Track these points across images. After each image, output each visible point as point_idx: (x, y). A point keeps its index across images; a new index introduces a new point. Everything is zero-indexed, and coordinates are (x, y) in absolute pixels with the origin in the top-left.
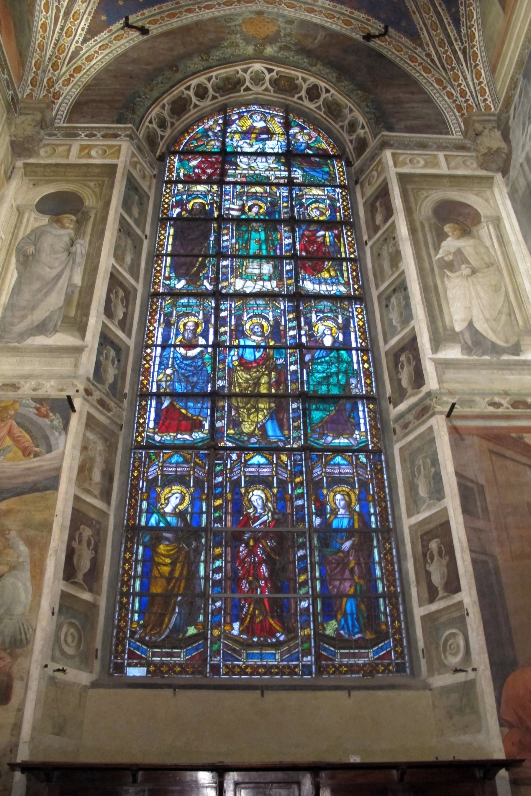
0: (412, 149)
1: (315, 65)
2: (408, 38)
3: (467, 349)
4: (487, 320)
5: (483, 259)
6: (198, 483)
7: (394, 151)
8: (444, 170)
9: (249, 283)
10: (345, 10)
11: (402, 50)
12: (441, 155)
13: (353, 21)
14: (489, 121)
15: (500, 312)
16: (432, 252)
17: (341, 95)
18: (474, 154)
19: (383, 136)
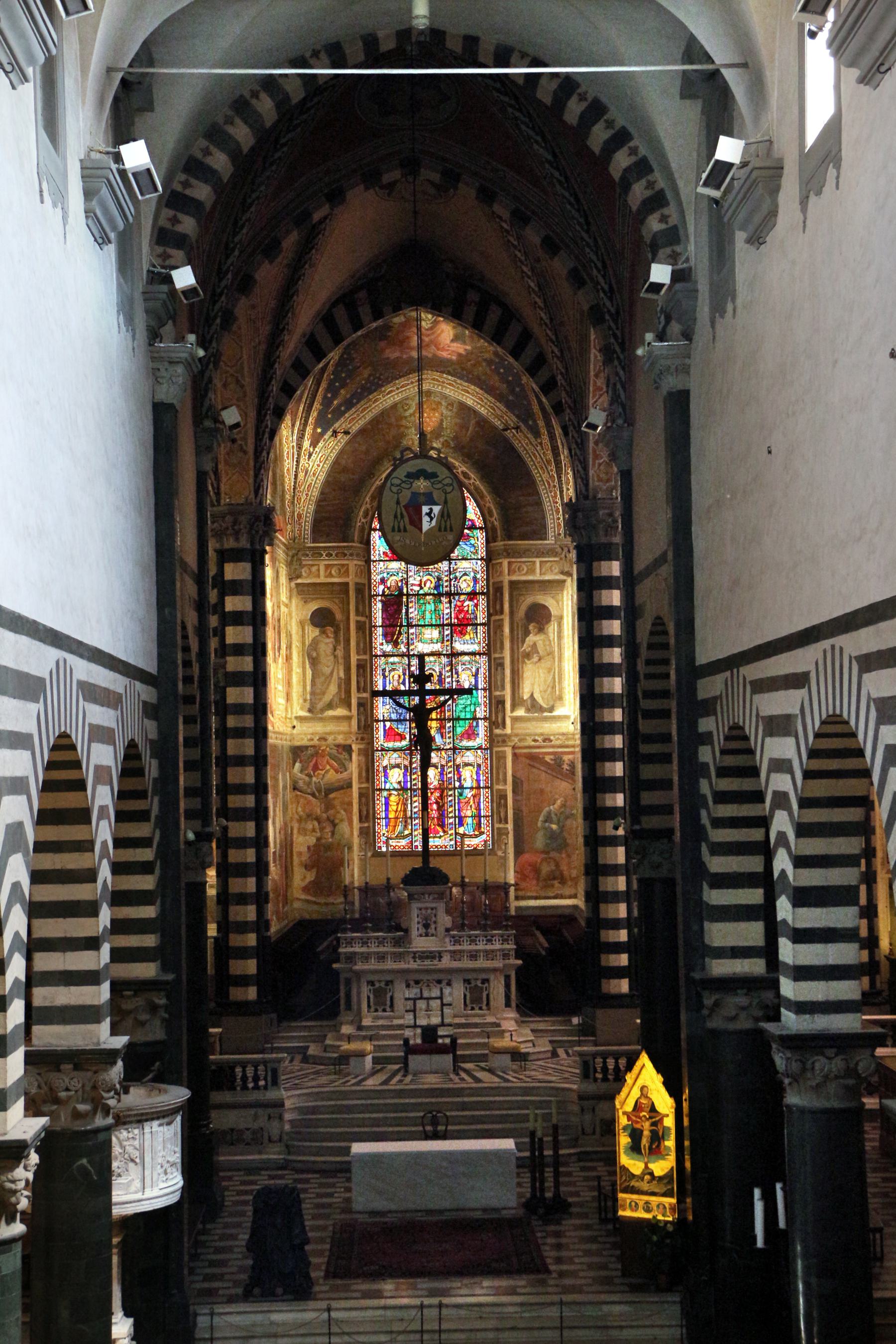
3: (528, 710)
6: (405, 767)
8: (537, 577)
9: (426, 646)
12: (538, 560)
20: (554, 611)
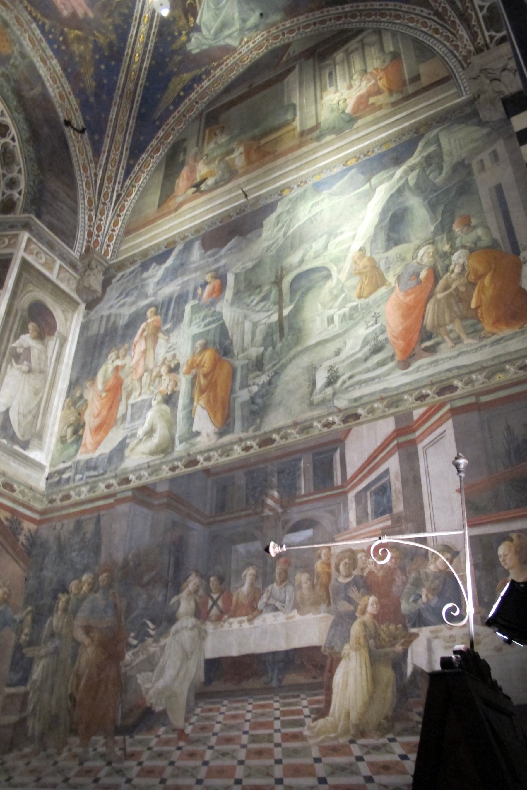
0: (43, 244)
1: (19, 114)
2: (92, 149)
4: (19, 413)
5: (40, 365)
7: (32, 237)
8: (53, 276)
10: (68, 88)
11: (82, 155)
12: (58, 262)
13: (66, 99)
14: (102, 264)
15: (30, 412)
16: (12, 338)
17: (21, 153)
18: (78, 277)
19: (30, 218)
20: (60, 327)
